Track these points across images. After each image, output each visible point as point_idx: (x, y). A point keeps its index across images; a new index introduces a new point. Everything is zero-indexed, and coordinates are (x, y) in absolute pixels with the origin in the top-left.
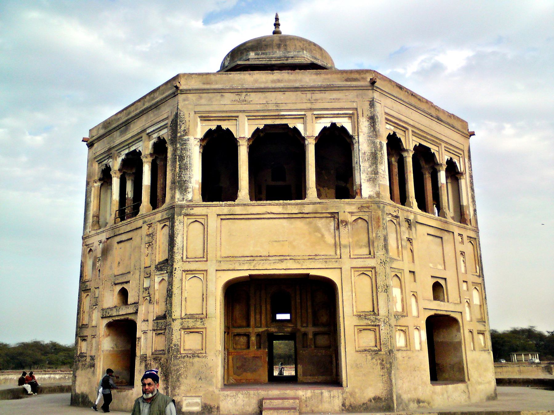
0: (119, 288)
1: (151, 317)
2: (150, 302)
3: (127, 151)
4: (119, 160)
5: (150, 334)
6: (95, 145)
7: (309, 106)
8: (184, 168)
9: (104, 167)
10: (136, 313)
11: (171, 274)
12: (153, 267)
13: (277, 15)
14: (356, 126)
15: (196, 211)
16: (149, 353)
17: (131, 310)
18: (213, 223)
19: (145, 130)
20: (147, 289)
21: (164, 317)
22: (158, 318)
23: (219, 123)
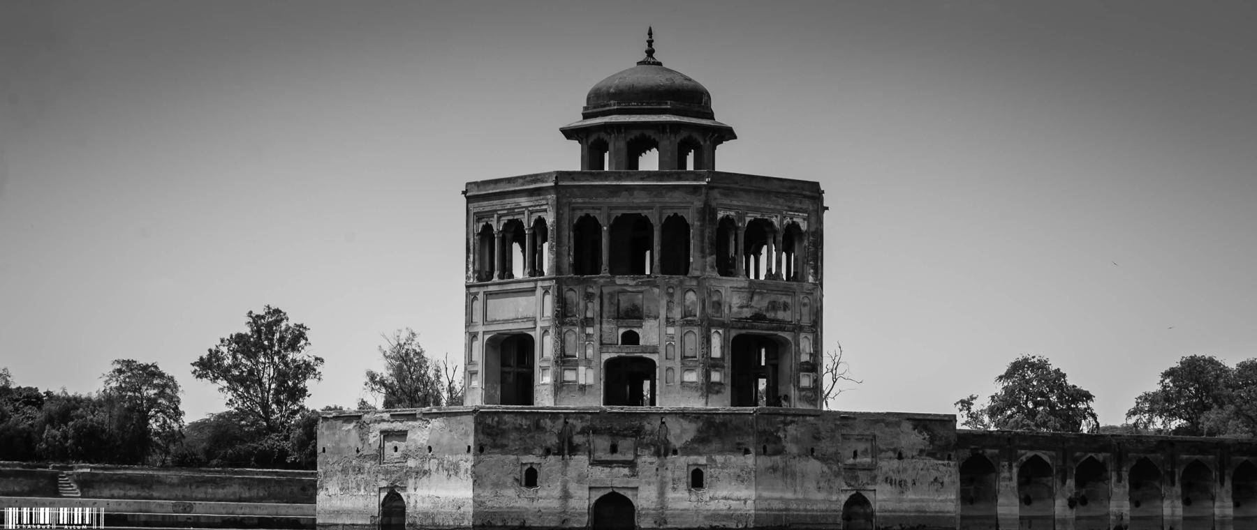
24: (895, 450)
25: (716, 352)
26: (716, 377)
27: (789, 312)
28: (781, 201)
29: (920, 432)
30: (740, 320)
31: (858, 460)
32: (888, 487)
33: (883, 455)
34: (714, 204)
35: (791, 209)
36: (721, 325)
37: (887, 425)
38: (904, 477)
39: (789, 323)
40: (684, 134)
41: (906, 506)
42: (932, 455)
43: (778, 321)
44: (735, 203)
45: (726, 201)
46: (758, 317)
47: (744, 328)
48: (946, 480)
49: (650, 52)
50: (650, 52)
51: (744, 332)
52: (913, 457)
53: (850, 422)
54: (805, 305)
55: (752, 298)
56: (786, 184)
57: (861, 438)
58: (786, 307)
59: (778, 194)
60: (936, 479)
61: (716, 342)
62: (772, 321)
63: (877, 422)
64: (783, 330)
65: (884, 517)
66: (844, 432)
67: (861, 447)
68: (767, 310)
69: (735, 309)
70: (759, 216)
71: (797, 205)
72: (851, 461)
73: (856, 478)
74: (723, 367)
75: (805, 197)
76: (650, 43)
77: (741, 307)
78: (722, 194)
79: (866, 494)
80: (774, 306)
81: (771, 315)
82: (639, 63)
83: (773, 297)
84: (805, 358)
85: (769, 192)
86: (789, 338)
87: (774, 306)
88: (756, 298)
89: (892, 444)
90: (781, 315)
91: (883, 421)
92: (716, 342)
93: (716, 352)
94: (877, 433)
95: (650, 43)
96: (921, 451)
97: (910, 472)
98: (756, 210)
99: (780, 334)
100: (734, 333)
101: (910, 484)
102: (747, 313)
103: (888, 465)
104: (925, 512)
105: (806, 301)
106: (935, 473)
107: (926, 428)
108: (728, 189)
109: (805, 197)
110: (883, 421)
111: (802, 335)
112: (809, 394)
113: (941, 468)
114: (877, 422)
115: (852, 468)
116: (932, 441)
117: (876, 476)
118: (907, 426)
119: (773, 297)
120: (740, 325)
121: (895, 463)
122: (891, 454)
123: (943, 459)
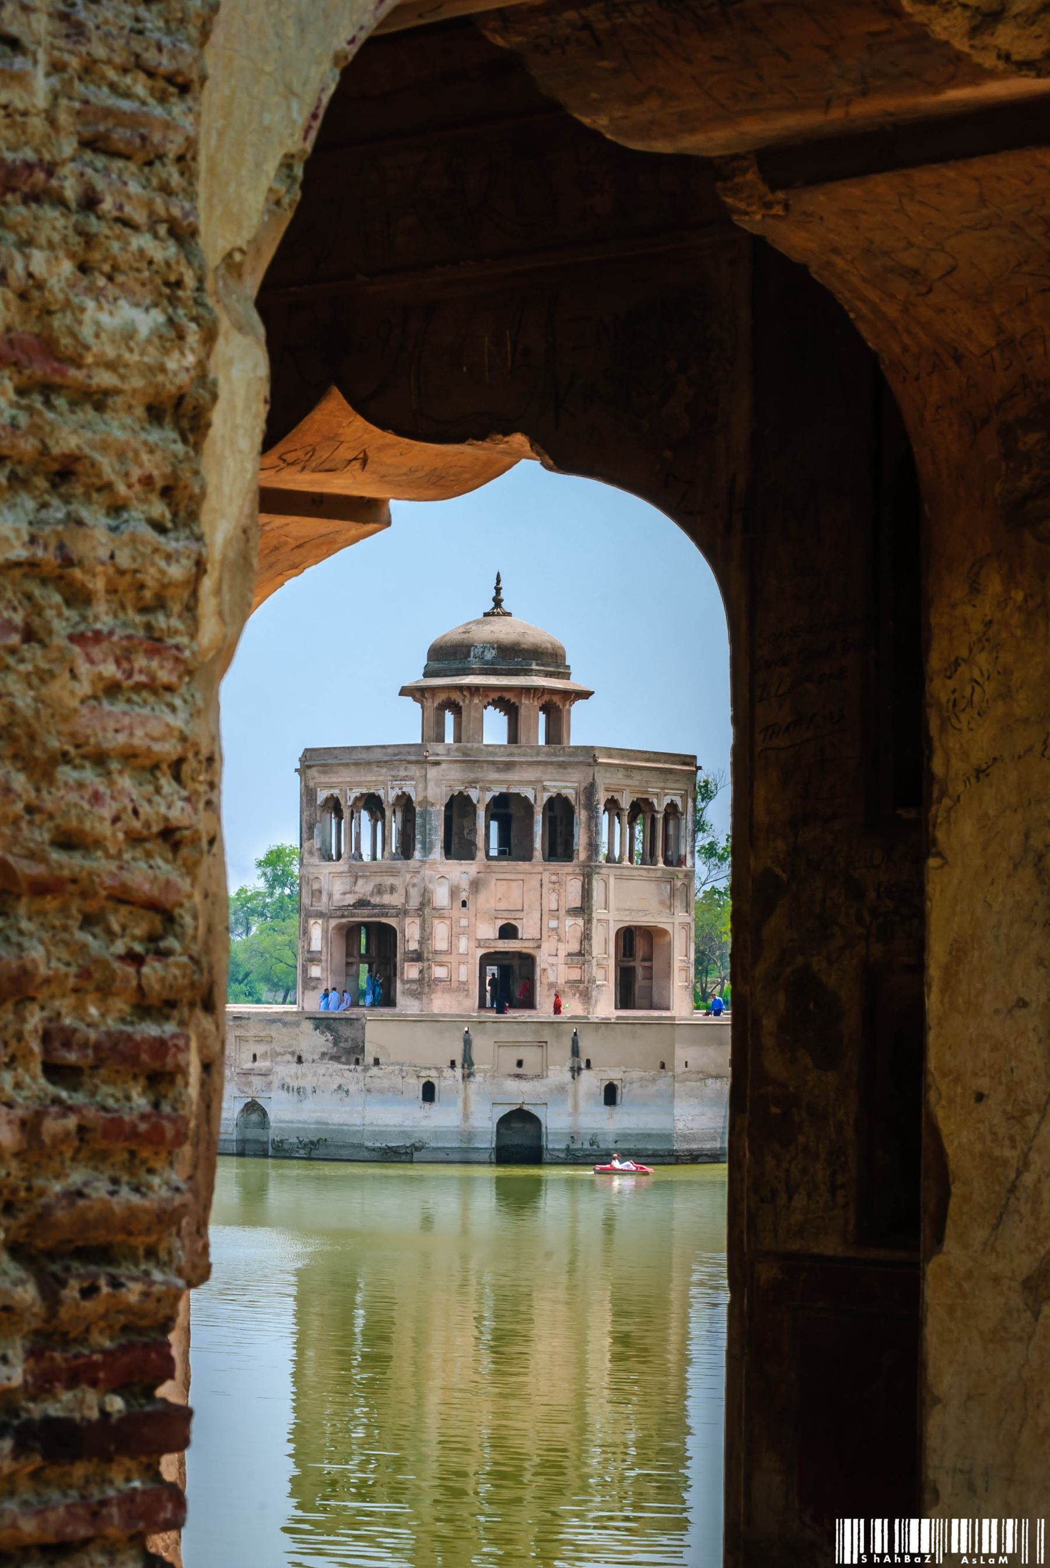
0: (500, 923)
1: (562, 953)
2: (559, 940)
3: (504, 791)
4: (488, 797)
5: (562, 968)
6: (444, 766)
7: (662, 785)
8: (598, 833)
9: (456, 794)
10: (539, 947)
11: (589, 921)
12: (562, 912)
13: (498, 575)
14: (685, 806)
15: (604, 871)
16: (561, 981)
17: (531, 944)
18: (612, 881)
19: (542, 782)
20: (553, 929)
21: (580, 954)
22: (569, 955)
23: (612, 794)
24: (293, 1053)
25: (316, 944)
26: (315, 971)
27: (395, 895)
28: (384, 771)
29: (323, 1033)
30: (339, 908)
31: (257, 1064)
32: (284, 1094)
33: (279, 1059)
34: (311, 784)
35: (395, 778)
36: (320, 915)
37: (285, 1024)
38: (302, 1083)
39: (394, 907)
40: (442, 697)
41: (304, 1116)
42: (336, 1058)
43: (383, 906)
44: (334, 780)
45: (324, 779)
46: (362, 903)
47: (343, 916)
48: (353, 1088)
49: (498, 601)
50: (498, 601)
51: (344, 920)
52: (313, 1061)
53: (244, 1022)
54: (414, 885)
55: (355, 883)
56: (389, 750)
57: (260, 1040)
58: (392, 889)
59: (379, 763)
60: (340, 1087)
61: (316, 931)
62: (375, 906)
63: (274, 1021)
64: (386, 915)
65: (281, 1129)
66: (238, 1033)
67: (260, 1049)
68: (372, 894)
69: (337, 896)
70: (365, 791)
71: (402, 773)
72: (248, 1065)
73: (249, 1084)
74: (320, 961)
75: (410, 762)
76: (498, 590)
77: (344, 894)
78: (320, 772)
79: (259, 1101)
80: (379, 890)
81: (376, 900)
82: (486, 615)
83: (378, 880)
84: (413, 946)
85: (369, 763)
86: (394, 925)
87: (379, 890)
88: (360, 882)
89: (290, 1046)
90: (387, 899)
91: (280, 1021)
92: (316, 931)
93: (316, 944)
94: (273, 1034)
95: (498, 590)
96: (324, 1054)
97: (310, 1078)
98: (359, 784)
99: (384, 920)
100: (333, 923)
101: (309, 1090)
102: (350, 900)
103: (286, 1070)
104: (327, 1124)
105: (415, 881)
106: (339, 1080)
107: (329, 1028)
108: (324, 765)
109: (410, 762)
110: (280, 1021)
111: (408, 920)
112: (414, 987)
113: (347, 1074)
114: (274, 1021)
115: (247, 1073)
116: (336, 1043)
117: (270, 1083)
118: (308, 1026)
119: (378, 880)
120: (339, 913)
121: (294, 1067)
122: (289, 1057)
123: (348, 1063)
